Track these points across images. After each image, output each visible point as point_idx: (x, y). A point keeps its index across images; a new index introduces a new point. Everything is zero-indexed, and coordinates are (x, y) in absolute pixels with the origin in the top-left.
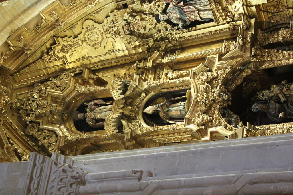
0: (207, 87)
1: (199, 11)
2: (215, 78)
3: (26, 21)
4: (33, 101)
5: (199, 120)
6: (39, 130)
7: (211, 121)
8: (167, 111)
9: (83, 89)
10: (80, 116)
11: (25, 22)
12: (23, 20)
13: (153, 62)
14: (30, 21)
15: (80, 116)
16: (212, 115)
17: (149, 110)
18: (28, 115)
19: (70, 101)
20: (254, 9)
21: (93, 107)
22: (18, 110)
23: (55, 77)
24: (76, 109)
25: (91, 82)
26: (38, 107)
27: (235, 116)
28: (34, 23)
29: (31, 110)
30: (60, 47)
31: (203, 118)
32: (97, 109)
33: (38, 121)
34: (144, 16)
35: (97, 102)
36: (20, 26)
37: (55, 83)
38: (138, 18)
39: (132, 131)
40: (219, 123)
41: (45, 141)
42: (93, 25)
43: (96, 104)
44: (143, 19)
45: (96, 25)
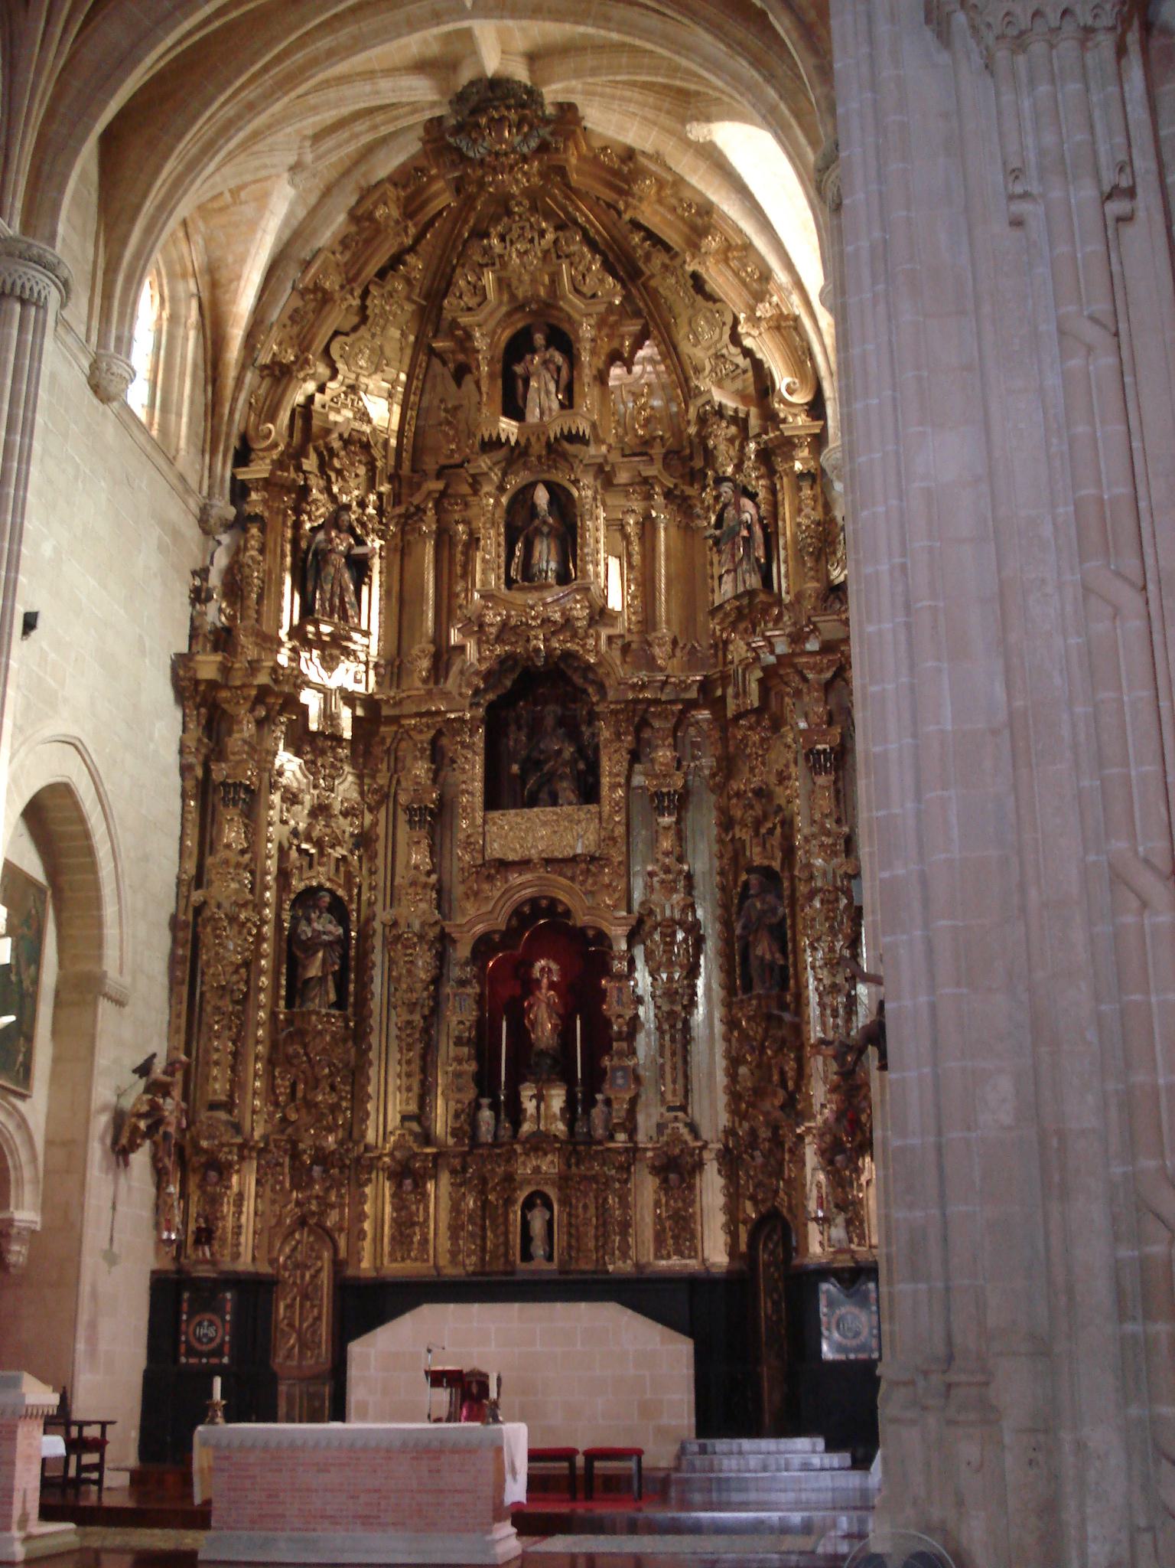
0: (555, 623)
1: (735, 571)
2: (574, 635)
3: (694, 180)
4: (532, 241)
5: (490, 617)
6: (481, 266)
7: (487, 642)
8: (542, 533)
9: (586, 331)
10: (539, 339)
11: (688, 178)
12: (695, 171)
13: (655, 477)
14: (694, 188)
15: (539, 339)
16: (499, 639)
17: (542, 496)
18: (502, 238)
19: (561, 309)
20: (719, 692)
21: (552, 367)
22: (509, 213)
23: (608, 267)
24: (555, 322)
25: (615, 344)
26: (521, 254)
27: (508, 683)
28: (698, 199)
29: (512, 243)
30: (667, 261)
31: (491, 625)
32: (548, 376)
33: (497, 261)
34: (737, 443)
35: (564, 373)
36: (678, 169)
37: (589, 269)
38: (733, 429)
39: (485, 474)
40: (485, 659)
41: (462, 283)
42: (724, 324)
43: (559, 369)
44: (731, 441)
45: (727, 331)
